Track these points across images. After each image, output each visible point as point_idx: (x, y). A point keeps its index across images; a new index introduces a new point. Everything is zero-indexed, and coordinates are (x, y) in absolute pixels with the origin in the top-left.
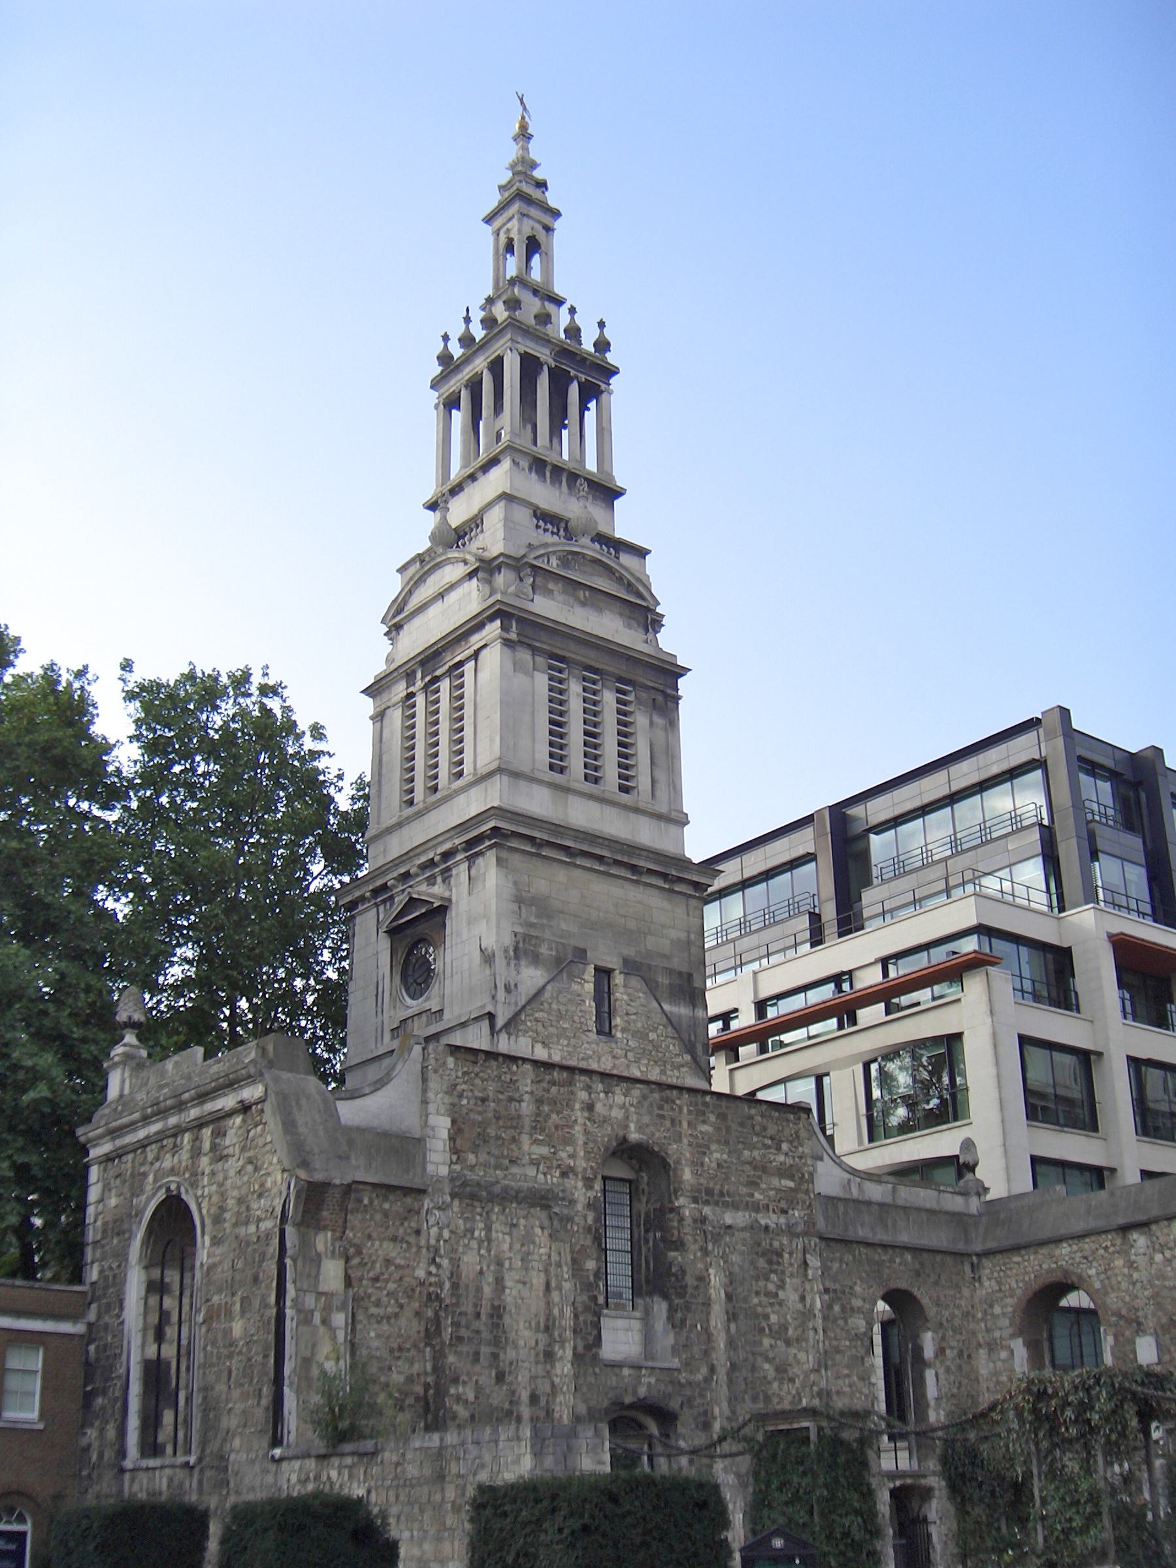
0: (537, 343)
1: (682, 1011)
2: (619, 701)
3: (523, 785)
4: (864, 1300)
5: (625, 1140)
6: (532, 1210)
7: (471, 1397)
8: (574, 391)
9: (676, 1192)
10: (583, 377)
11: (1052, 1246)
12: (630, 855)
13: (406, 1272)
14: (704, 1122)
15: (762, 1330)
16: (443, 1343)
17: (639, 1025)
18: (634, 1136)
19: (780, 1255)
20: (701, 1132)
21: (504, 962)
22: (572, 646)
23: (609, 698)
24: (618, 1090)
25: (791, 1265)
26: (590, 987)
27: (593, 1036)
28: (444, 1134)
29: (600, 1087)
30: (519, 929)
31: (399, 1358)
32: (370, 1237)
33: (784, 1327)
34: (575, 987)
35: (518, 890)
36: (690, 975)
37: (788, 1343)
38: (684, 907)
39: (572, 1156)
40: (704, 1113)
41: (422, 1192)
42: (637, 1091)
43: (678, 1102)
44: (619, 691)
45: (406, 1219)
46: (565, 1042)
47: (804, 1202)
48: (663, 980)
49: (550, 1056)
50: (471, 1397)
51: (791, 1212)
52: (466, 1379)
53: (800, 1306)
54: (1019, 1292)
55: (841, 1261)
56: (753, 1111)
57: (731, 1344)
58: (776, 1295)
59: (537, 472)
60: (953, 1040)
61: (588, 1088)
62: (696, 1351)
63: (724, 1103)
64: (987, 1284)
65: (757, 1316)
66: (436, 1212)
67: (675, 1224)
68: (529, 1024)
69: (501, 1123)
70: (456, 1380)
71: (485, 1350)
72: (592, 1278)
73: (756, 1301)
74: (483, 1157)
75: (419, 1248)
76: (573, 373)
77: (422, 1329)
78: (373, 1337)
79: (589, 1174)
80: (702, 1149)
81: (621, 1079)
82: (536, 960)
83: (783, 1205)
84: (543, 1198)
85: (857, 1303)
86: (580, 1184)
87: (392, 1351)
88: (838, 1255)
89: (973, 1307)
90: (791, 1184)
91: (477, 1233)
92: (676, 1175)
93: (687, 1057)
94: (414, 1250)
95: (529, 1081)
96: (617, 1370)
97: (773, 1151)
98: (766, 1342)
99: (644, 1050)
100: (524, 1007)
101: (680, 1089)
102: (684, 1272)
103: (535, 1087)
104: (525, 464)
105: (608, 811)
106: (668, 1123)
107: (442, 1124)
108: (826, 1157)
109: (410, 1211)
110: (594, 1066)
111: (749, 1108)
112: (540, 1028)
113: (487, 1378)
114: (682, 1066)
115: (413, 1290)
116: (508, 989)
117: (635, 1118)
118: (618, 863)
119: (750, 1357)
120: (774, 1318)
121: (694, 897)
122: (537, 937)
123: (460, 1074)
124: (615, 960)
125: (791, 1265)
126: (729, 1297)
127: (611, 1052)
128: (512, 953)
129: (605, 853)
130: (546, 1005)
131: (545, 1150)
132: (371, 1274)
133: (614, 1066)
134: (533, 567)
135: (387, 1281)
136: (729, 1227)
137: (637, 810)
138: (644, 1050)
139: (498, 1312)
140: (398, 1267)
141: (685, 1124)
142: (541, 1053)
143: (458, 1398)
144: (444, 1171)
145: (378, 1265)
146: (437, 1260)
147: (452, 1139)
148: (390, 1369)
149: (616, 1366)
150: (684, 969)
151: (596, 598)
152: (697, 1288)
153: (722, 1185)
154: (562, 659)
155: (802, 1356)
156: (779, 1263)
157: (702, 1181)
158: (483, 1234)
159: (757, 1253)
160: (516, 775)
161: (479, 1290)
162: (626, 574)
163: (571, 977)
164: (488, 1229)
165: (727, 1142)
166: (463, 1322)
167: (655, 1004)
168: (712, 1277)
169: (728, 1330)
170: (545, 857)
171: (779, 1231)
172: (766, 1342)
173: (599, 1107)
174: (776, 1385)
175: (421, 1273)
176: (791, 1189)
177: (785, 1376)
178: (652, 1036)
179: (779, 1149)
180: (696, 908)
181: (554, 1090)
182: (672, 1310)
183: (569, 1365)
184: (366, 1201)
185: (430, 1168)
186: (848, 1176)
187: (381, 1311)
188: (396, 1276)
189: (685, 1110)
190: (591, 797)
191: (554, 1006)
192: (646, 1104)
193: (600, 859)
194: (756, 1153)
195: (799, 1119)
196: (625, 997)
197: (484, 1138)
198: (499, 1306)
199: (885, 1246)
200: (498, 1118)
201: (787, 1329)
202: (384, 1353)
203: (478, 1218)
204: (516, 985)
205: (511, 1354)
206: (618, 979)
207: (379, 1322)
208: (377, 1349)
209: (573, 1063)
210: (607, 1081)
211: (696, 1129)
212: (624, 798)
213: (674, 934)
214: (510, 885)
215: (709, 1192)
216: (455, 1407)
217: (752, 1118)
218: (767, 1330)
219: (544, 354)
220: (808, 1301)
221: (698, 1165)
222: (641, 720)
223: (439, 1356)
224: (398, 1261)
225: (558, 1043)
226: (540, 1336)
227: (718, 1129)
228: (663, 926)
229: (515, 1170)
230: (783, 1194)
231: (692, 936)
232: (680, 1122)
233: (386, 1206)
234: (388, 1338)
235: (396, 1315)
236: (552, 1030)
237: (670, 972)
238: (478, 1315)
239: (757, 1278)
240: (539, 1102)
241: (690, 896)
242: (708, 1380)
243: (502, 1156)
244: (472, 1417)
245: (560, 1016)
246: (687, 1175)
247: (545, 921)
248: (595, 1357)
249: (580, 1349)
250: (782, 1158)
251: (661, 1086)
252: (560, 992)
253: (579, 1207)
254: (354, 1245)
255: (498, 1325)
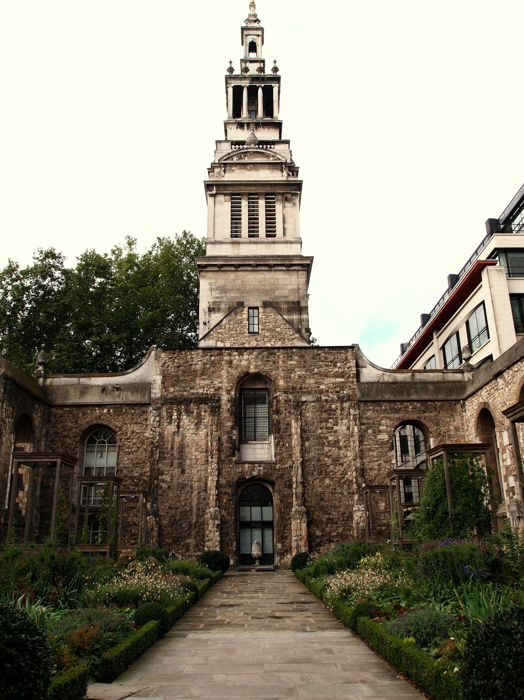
0: (241, 80)
1: (295, 317)
2: (266, 203)
3: (218, 246)
4: (387, 426)
5: (247, 374)
6: (200, 406)
7: (169, 480)
8: (260, 92)
9: (275, 390)
10: (263, 85)
11: (480, 391)
12: (264, 260)
13: (141, 434)
14: (292, 360)
15: (323, 444)
16: (155, 460)
17: (271, 326)
18: (252, 370)
19: (335, 411)
20: (290, 365)
21: (203, 314)
22: (243, 188)
23: (262, 203)
24: (245, 354)
25: (341, 414)
26: (245, 316)
27: (247, 334)
28: (159, 382)
29: (236, 353)
30: (211, 300)
31: (137, 467)
32: (125, 424)
33: (337, 442)
34: (239, 317)
35: (210, 286)
36: (299, 302)
37: (340, 448)
38: (296, 275)
39: (219, 383)
40: (291, 356)
41: (149, 404)
42: (255, 353)
43: (278, 354)
44: (266, 199)
45: (141, 415)
46: (233, 339)
47: (350, 387)
48: (284, 306)
49: (225, 345)
50: (169, 480)
51: (341, 392)
52: (166, 472)
53: (346, 432)
54: (475, 414)
55: (373, 410)
56: (320, 352)
57: (303, 451)
58: (332, 428)
59: (240, 128)
60: (483, 303)
61: (230, 355)
62: (285, 455)
63: (303, 351)
64: (468, 413)
65: (321, 438)
66: (154, 411)
67: (275, 403)
68: (215, 335)
69: (186, 374)
70: (162, 474)
71: (176, 462)
72: (229, 430)
73: (320, 431)
74: (177, 389)
75: (147, 426)
76: (258, 85)
77: (147, 455)
78: (126, 461)
79: (229, 388)
80: (291, 371)
81: (246, 349)
82: (219, 310)
83: (338, 389)
84: (203, 400)
85: (381, 428)
86: (224, 393)
87: (134, 464)
88: (371, 408)
89: (463, 424)
90: (343, 380)
91: (173, 417)
92: (275, 384)
93: (297, 335)
94: (145, 426)
95: (200, 356)
96: (241, 465)
97: (332, 367)
98: (326, 449)
99: (273, 336)
100: (212, 329)
101: (279, 348)
102: (278, 422)
103: (203, 358)
104: (235, 127)
105: (260, 246)
106: (271, 363)
107: (159, 379)
108: (369, 366)
109: (144, 412)
110: (247, 346)
111: (318, 350)
112: (220, 335)
113: (177, 471)
114: (294, 339)
115: (144, 441)
116: (205, 324)
117: (253, 363)
118: (257, 265)
119: (316, 455)
120: (330, 438)
121: (301, 270)
122: (219, 302)
123: (167, 359)
124: (259, 303)
125: (341, 414)
126: (303, 431)
127: (256, 339)
128: (207, 310)
129: (252, 263)
130: (223, 327)
131: (207, 382)
132: (126, 437)
133: (257, 345)
134: (223, 164)
135: (133, 439)
136: (305, 402)
137: (274, 243)
138: (273, 336)
139: (182, 447)
140: (137, 433)
141: (281, 362)
142: (220, 345)
143: (163, 481)
144: (159, 395)
145: (129, 433)
146: (153, 429)
147: (163, 383)
148: (132, 471)
149: (241, 462)
150: (296, 300)
151: (256, 165)
152: (285, 429)
153: (301, 385)
154: (239, 194)
155: (349, 454)
156: (335, 415)
157: (289, 384)
158: (176, 417)
159: (322, 412)
160: (215, 243)
161: (173, 439)
162: (270, 153)
163: (236, 314)
164: (179, 414)
165: (304, 367)
166: (166, 451)
167: (280, 317)
168: (293, 424)
169: (302, 445)
170: (223, 271)
171: (333, 401)
172: (326, 449)
173: (234, 362)
174: (331, 467)
175: (147, 435)
176: (342, 382)
177: (338, 462)
178: (278, 329)
179: (335, 366)
180: (303, 274)
181: (213, 358)
182: (275, 439)
183: (215, 465)
184: (124, 411)
185: (153, 395)
186: (382, 372)
187: (130, 450)
188: (137, 437)
189: (281, 357)
190: (251, 243)
191: (227, 326)
192: (260, 356)
193: (250, 265)
194: (320, 369)
195: (348, 351)
196: (264, 317)
197: (178, 381)
198: (183, 444)
199: (402, 402)
200: (185, 372)
201: (338, 442)
202: (130, 465)
203: (174, 411)
204: (209, 322)
205: (188, 462)
206: (261, 310)
207: (129, 454)
208: (127, 464)
209: (236, 346)
210: (239, 351)
211: (287, 363)
212: (270, 239)
213: (290, 287)
214: (207, 284)
215: (294, 388)
216: (161, 484)
217: (320, 355)
218: (327, 444)
219: (246, 83)
220: (351, 429)
221: (287, 378)
222: (278, 207)
223: (152, 464)
224: (137, 431)
225: (229, 340)
226: (204, 454)
227: (299, 362)
228: (285, 285)
229: (192, 391)
230: (337, 385)
231: (300, 286)
232: (278, 362)
233: (133, 411)
234: (132, 460)
235: (136, 451)
236: (228, 336)
237: (288, 303)
238: (172, 448)
239: (321, 422)
240: (204, 364)
241: (298, 270)
242: (291, 467)
243: (187, 387)
244: (169, 487)
245: (230, 329)
246: (281, 383)
247: (223, 295)
248: (231, 461)
249: (223, 457)
250: (337, 369)
251: (267, 348)
252: (230, 321)
253: (223, 402)
254: (119, 427)
255: (182, 451)
